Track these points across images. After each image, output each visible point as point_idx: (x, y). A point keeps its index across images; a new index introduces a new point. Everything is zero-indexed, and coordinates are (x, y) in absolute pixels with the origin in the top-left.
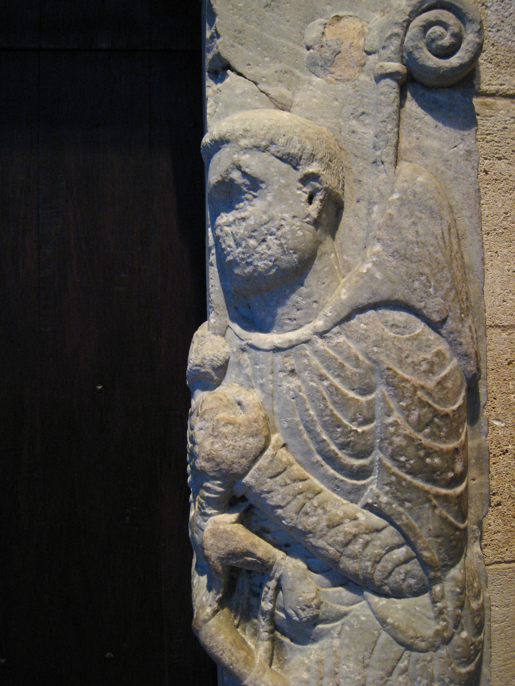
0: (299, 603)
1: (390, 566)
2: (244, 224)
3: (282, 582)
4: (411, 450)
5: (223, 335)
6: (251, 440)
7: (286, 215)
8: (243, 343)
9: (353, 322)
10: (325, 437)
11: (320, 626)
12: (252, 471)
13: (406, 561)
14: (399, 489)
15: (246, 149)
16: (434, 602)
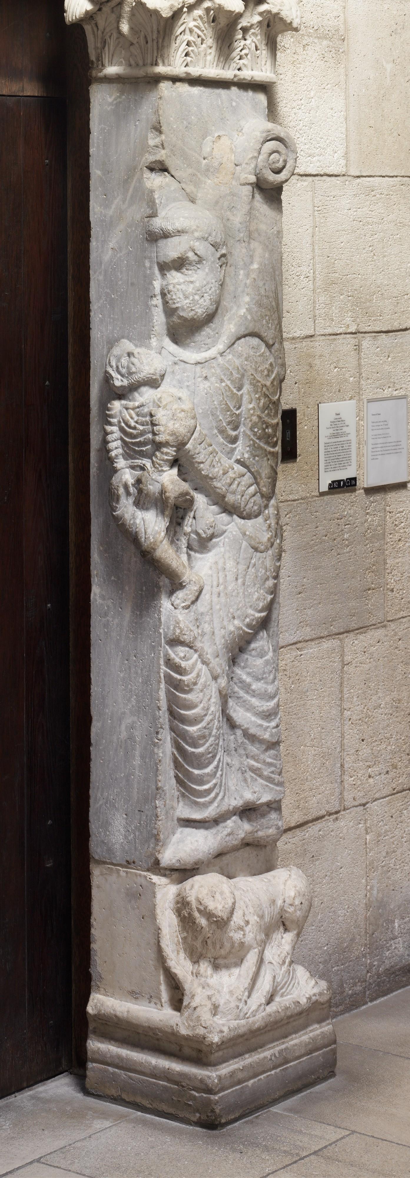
0: (207, 525)
1: (248, 497)
2: (192, 286)
4: (260, 424)
8: (176, 359)
9: (235, 345)
11: (214, 540)
12: (191, 441)
13: (254, 495)
15: (198, 239)
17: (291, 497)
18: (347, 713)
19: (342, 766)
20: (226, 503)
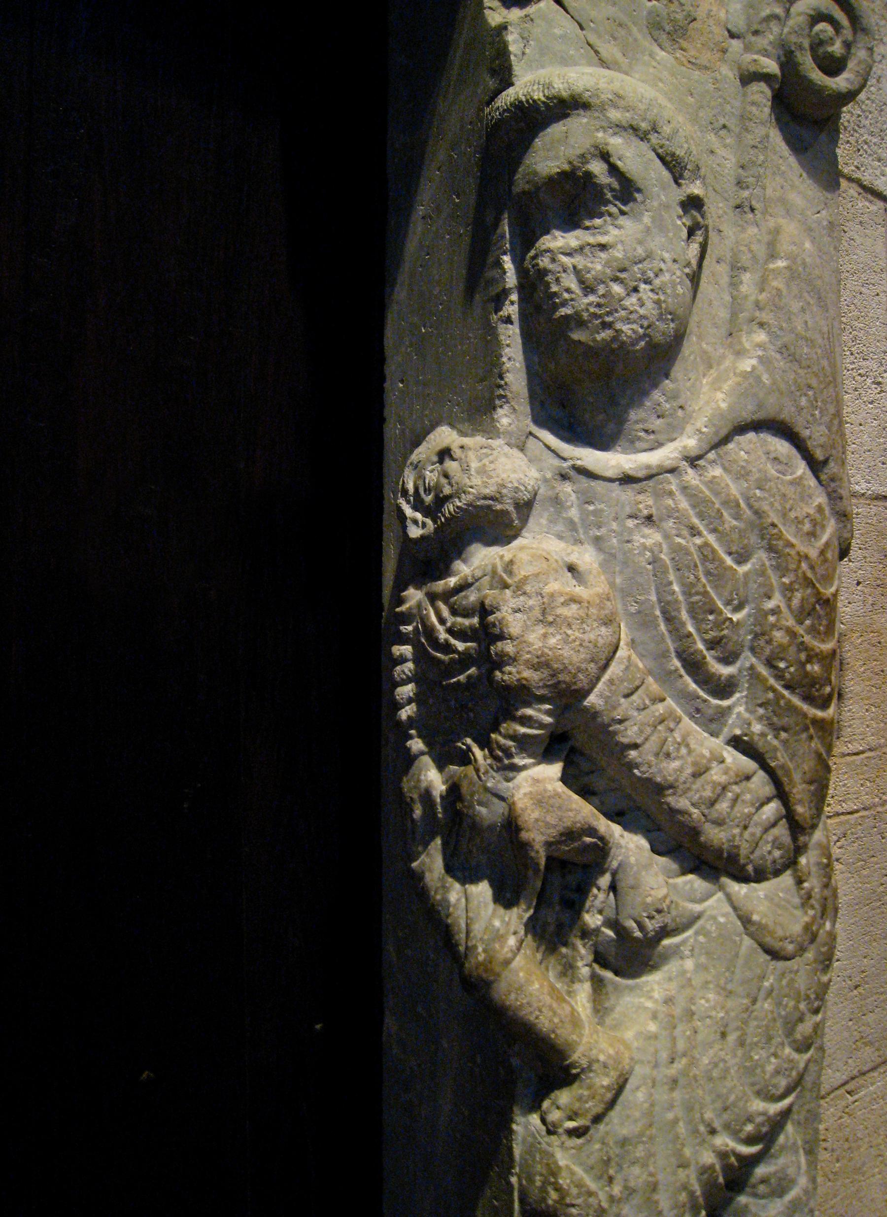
0: (646, 906)
2: (603, 255)
3: (620, 876)
4: (792, 650)
5: (522, 449)
6: (603, 629)
7: (666, 256)
8: (565, 465)
9: (731, 446)
10: (691, 629)
11: (666, 942)
12: (600, 685)
13: (774, 825)
15: (619, 128)
16: (799, 882)
17: (846, 807)
20: (705, 847)
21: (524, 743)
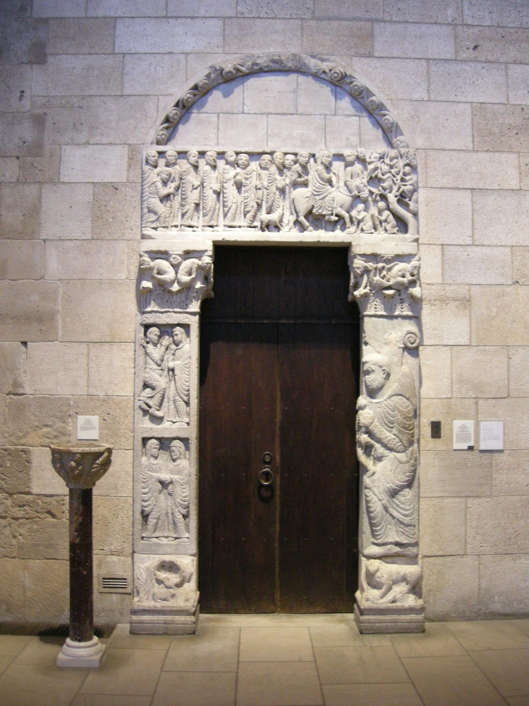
14: (400, 431)
18: (468, 524)
19: (466, 541)
21: (362, 432)
